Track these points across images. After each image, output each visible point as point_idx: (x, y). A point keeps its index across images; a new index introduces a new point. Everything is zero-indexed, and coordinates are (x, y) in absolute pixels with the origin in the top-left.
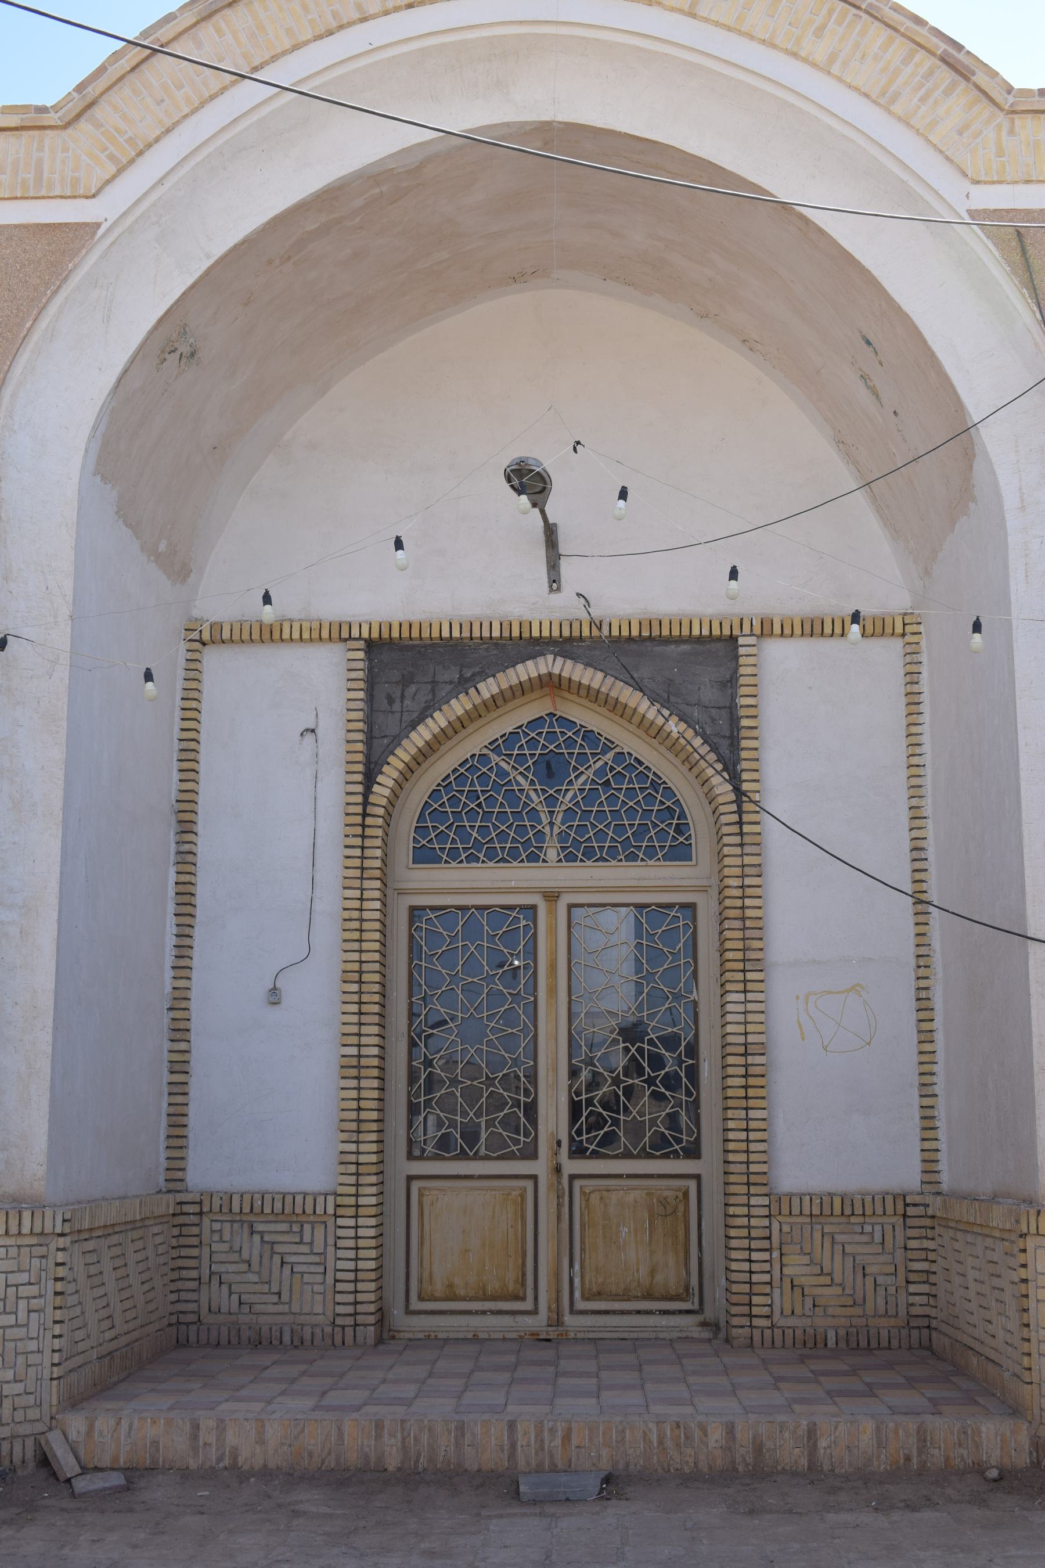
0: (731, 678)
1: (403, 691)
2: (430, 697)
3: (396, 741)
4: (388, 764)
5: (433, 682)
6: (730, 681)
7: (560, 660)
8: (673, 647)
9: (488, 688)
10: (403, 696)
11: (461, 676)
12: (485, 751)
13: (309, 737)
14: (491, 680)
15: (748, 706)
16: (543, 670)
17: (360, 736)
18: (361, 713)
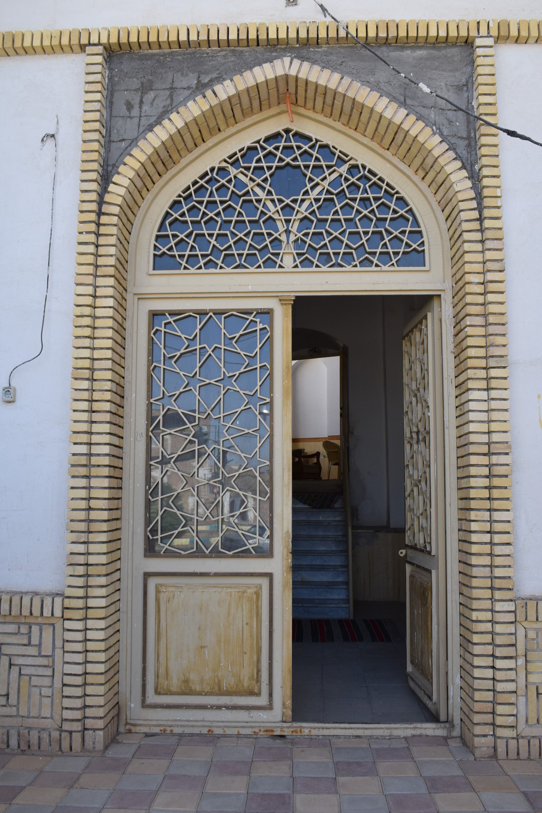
0: (467, 82)
1: (142, 97)
2: (169, 102)
3: (134, 142)
4: (125, 164)
5: (172, 88)
6: (466, 85)
7: (296, 63)
8: (409, 52)
9: (225, 90)
10: (141, 102)
11: (199, 82)
12: (224, 164)
13: (50, 142)
14: (228, 83)
15: (486, 104)
16: (280, 72)
17: (96, 136)
18: (98, 114)
